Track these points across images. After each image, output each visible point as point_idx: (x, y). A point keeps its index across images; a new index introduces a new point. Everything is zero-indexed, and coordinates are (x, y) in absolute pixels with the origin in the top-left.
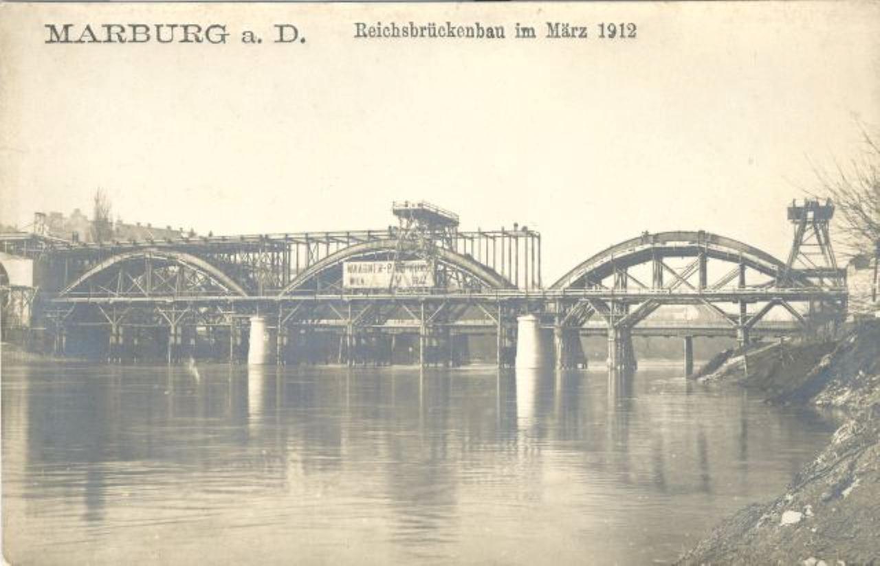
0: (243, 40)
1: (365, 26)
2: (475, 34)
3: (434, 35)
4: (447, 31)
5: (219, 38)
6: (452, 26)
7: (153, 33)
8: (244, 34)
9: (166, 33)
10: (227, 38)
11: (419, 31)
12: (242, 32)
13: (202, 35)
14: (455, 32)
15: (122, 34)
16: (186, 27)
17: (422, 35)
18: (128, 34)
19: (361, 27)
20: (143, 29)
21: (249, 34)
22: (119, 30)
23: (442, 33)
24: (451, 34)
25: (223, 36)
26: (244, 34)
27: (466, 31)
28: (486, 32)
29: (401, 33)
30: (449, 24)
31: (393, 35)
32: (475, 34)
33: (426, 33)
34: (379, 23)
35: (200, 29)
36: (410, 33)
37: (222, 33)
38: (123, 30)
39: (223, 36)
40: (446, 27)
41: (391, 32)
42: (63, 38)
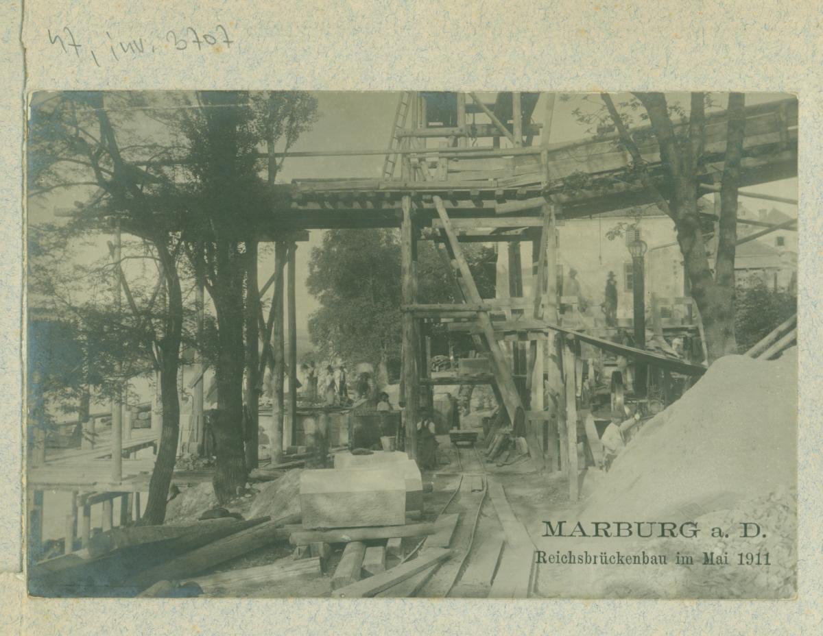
0: (713, 535)
1: (545, 554)
2: (641, 561)
3: (606, 563)
4: (616, 559)
5: (692, 533)
6: (621, 555)
7: (635, 528)
8: (713, 530)
9: (645, 530)
10: (698, 533)
11: (593, 558)
12: (711, 528)
13: (676, 531)
14: (624, 561)
15: (608, 530)
16: (663, 525)
17: (595, 563)
18: (613, 530)
19: (542, 554)
20: (627, 526)
21: (717, 530)
22: (606, 526)
23: (613, 560)
24: (620, 562)
25: (695, 533)
26: (713, 530)
27: (633, 558)
28: (650, 560)
29: (576, 561)
30: (618, 553)
31: (570, 562)
32: (641, 561)
33: (598, 560)
34: (558, 552)
35: (675, 526)
36: (584, 560)
37: (694, 529)
38: (609, 526)
39: (695, 533)
40: (616, 555)
41: (568, 559)
42: (557, 533)
